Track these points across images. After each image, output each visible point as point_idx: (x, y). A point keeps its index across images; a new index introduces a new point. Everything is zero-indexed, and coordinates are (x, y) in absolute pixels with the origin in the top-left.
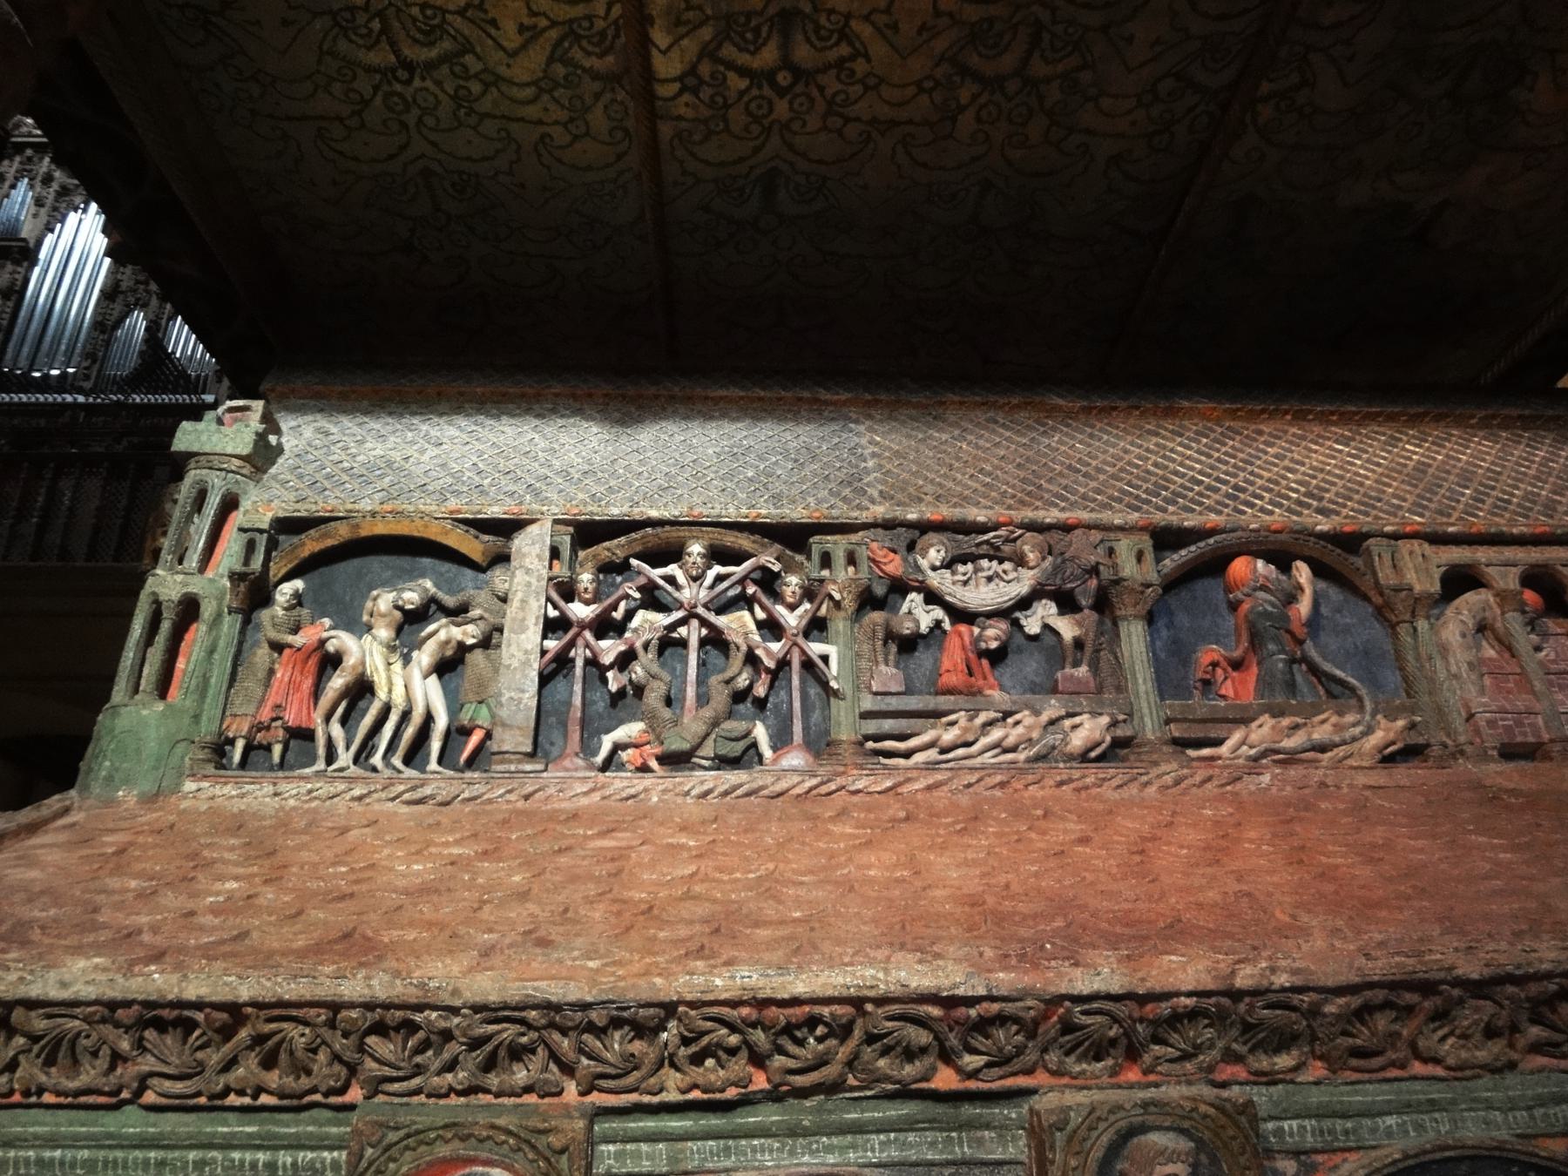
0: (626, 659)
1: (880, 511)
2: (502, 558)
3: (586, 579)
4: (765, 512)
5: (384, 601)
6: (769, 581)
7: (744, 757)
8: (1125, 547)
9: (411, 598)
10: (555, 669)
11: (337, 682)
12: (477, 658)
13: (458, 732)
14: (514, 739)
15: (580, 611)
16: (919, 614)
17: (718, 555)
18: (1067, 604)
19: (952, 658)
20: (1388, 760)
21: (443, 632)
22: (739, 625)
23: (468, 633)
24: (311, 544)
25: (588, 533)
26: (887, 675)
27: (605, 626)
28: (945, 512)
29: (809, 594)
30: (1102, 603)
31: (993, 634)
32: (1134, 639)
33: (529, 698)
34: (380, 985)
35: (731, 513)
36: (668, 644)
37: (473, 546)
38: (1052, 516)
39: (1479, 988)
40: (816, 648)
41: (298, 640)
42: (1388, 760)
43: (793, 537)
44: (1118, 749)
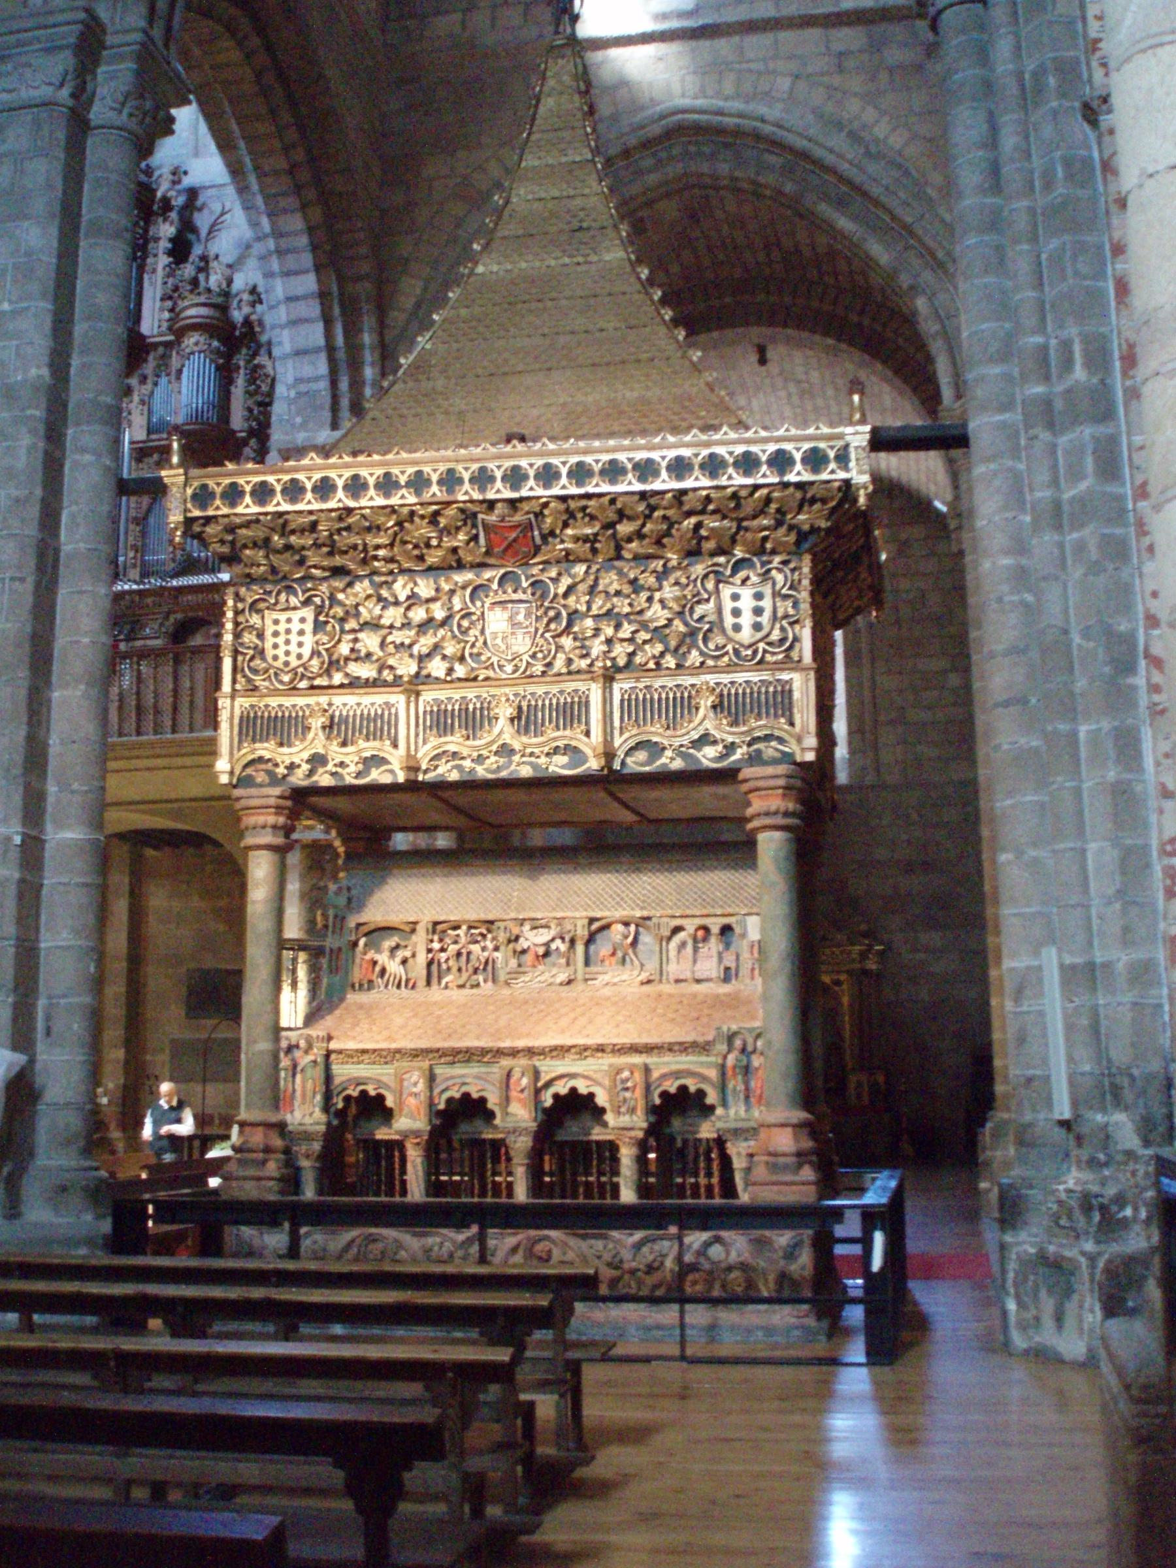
0: (447, 960)
1: (513, 915)
2: (413, 931)
3: (436, 938)
4: (483, 917)
5: (388, 943)
6: (484, 936)
7: (478, 985)
8: (580, 923)
9: (393, 944)
10: (430, 964)
11: (378, 969)
12: (411, 961)
13: (407, 981)
14: (422, 983)
15: (436, 946)
16: (523, 944)
17: (470, 928)
18: (563, 939)
19: (528, 958)
20: (642, 983)
21: (400, 954)
22: (475, 948)
23: (408, 953)
24: (365, 929)
25: (436, 924)
26: (513, 963)
27: (443, 950)
28: (533, 915)
29: (494, 939)
30: (573, 942)
31: (541, 951)
32: (580, 948)
33: (424, 972)
34: (394, 1046)
35: (473, 916)
36: (459, 954)
37: (407, 929)
38: (559, 915)
39: (574, 1046)
40: (496, 954)
41: (368, 957)
42: (642, 983)
43: (492, 922)
44: (569, 982)
